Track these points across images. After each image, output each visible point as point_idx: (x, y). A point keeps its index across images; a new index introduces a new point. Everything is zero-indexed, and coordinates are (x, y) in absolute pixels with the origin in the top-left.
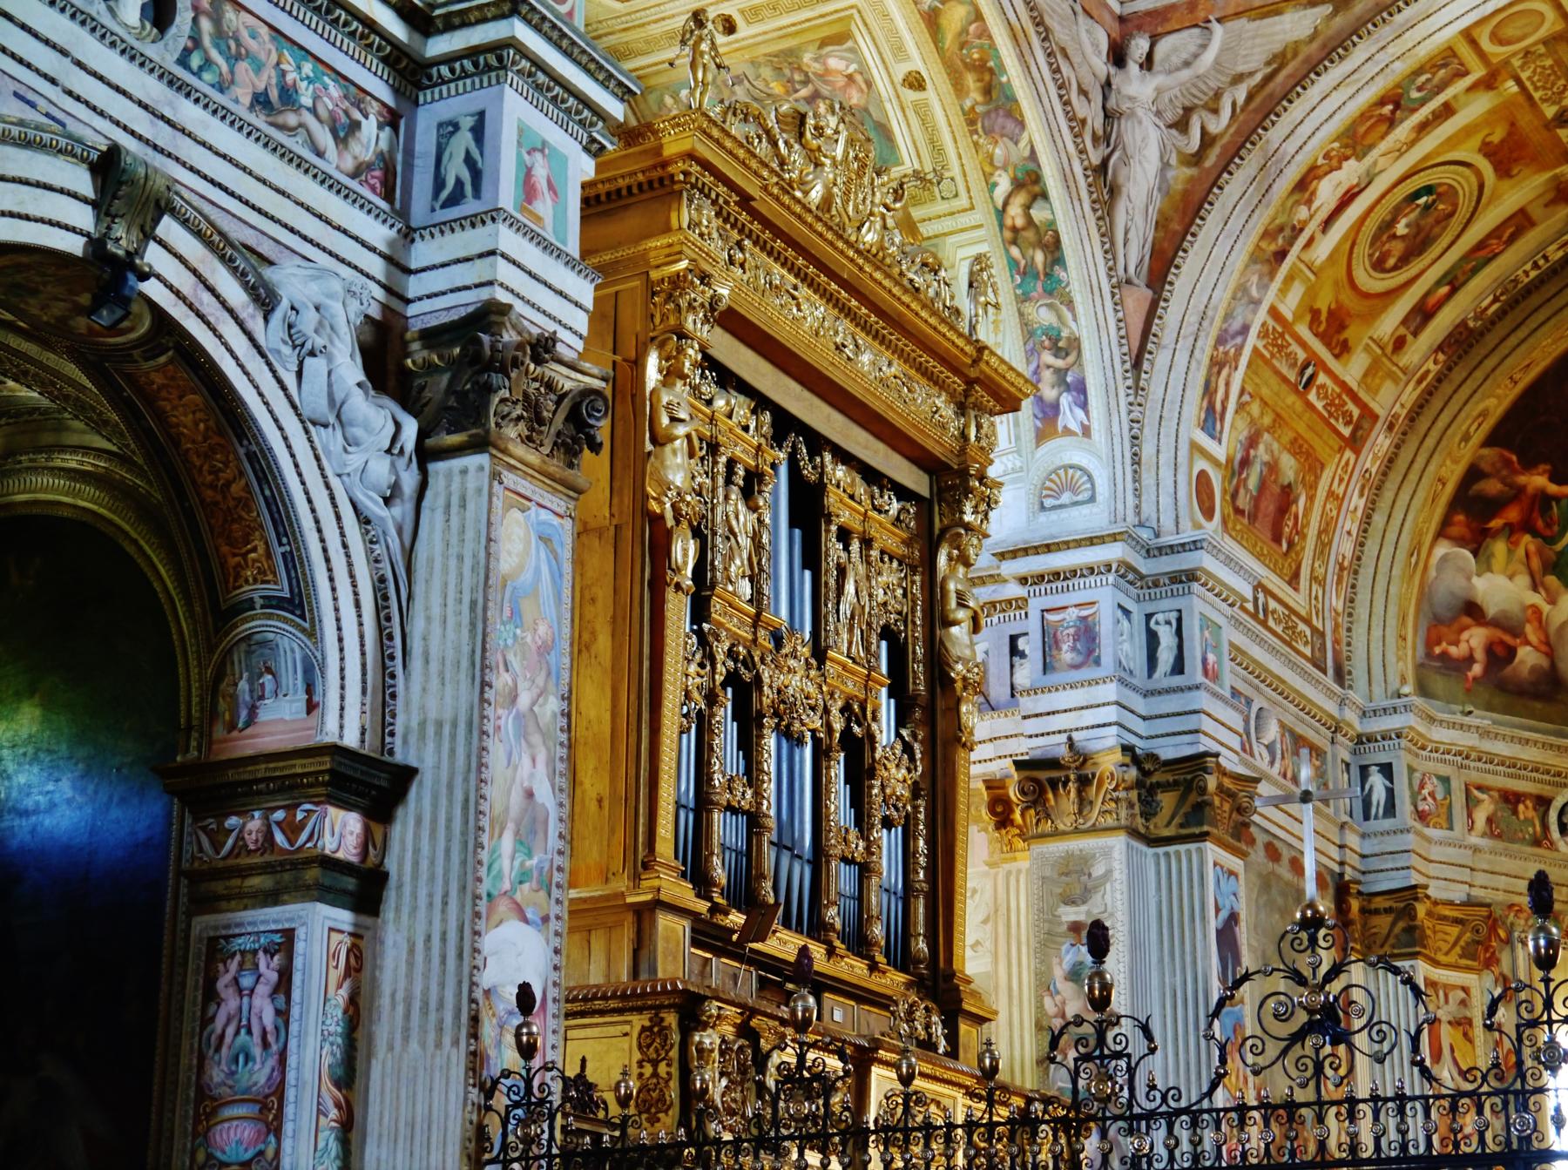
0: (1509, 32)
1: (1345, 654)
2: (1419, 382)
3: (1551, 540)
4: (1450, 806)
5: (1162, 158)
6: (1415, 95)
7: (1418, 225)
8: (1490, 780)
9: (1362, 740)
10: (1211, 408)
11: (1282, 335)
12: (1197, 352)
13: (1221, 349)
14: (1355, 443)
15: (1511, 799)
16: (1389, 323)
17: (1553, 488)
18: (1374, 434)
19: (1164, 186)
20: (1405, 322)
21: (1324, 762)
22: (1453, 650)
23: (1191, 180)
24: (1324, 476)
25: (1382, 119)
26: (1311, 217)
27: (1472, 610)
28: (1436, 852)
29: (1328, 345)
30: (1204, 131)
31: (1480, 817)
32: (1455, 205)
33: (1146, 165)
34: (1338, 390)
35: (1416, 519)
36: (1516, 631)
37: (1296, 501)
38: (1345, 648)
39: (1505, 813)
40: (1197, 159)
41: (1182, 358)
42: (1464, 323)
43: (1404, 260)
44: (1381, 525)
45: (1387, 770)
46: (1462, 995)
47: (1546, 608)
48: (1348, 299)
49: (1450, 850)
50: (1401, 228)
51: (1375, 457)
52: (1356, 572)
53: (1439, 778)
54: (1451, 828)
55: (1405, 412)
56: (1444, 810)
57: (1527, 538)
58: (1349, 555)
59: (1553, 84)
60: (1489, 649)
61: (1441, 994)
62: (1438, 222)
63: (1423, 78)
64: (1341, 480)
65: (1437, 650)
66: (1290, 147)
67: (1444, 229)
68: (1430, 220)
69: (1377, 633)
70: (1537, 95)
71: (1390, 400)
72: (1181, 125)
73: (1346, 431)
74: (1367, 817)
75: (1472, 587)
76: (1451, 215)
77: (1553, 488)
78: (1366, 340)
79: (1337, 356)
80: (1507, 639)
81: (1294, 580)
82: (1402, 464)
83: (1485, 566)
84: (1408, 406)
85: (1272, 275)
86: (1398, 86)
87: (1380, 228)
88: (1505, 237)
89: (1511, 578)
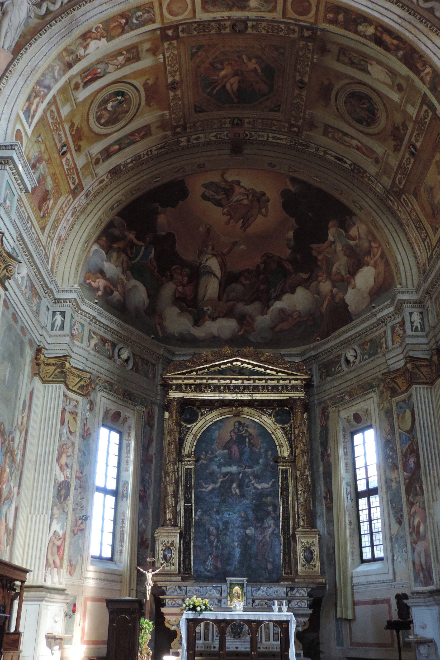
0: (174, 8)
1: (55, 270)
2: (101, 182)
3: (131, 259)
4: (83, 336)
5: (28, 14)
6: (135, 21)
7: (115, 109)
8: (97, 331)
9: (56, 301)
10: (29, 109)
11: (59, 123)
12: (28, 82)
13: (38, 87)
14: (74, 193)
15: (104, 340)
16: (97, 148)
17: (135, 241)
18: (81, 195)
19: (26, 24)
20: (101, 152)
21: (40, 302)
22: (93, 283)
23: (38, 24)
24: (62, 198)
25: (120, 25)
26: (85, 56)
27: (102, 272)
28: (75, 349)
29: (74, 142)
30: (47, 9)
31: (93, 343)
32: (129, 108)
33: (21, 12)
34: (73, 166)
35: (91, 229)
36: (115, 286)
37: (49, 199)
38: (55, 268)
39: (101, 344)
40: (43, 17)
41: (21, 82)
42: (119, 166)
43: (107, 124)
44: (77, 230)
45: (63, 314)
46: (76, 403)
47: (126, 281)
48: (85, 129)
49: (81, 350)
50: (109, 106)
51: (79, 205)
52: (64, 243)
53: (81, 324)
54: (82, 343)
55: (93, 193)
56: (80, 336)
57: (124, 255)
58: (63, 236)
59: (175, 66)
60: (105, 288)
61: (68, 401)
62: (122, 113)
63: (140, 13)
64: (66, 206)
65: (88, 281)
66: (83, 19)
67: (123, 117)
68: (119, 109)
69: (68, 265)
70: (168, 68)
71: (89, 184)
72: (39, 5)
73: (72, 187)
74: (52, 330)
75: (104, 265)
76: (127, 112)
77: (135, 241)
78: (86, 152)
79: (76, 151)
80: (112, 287)
81: (43, 229)
82: (88, 211)
83: (109, 259)
84: (95, 191)
85: (65, 72)
86: (129, 11)
87: (102, 101)
88: (141, 135)
89: (116, 267)
